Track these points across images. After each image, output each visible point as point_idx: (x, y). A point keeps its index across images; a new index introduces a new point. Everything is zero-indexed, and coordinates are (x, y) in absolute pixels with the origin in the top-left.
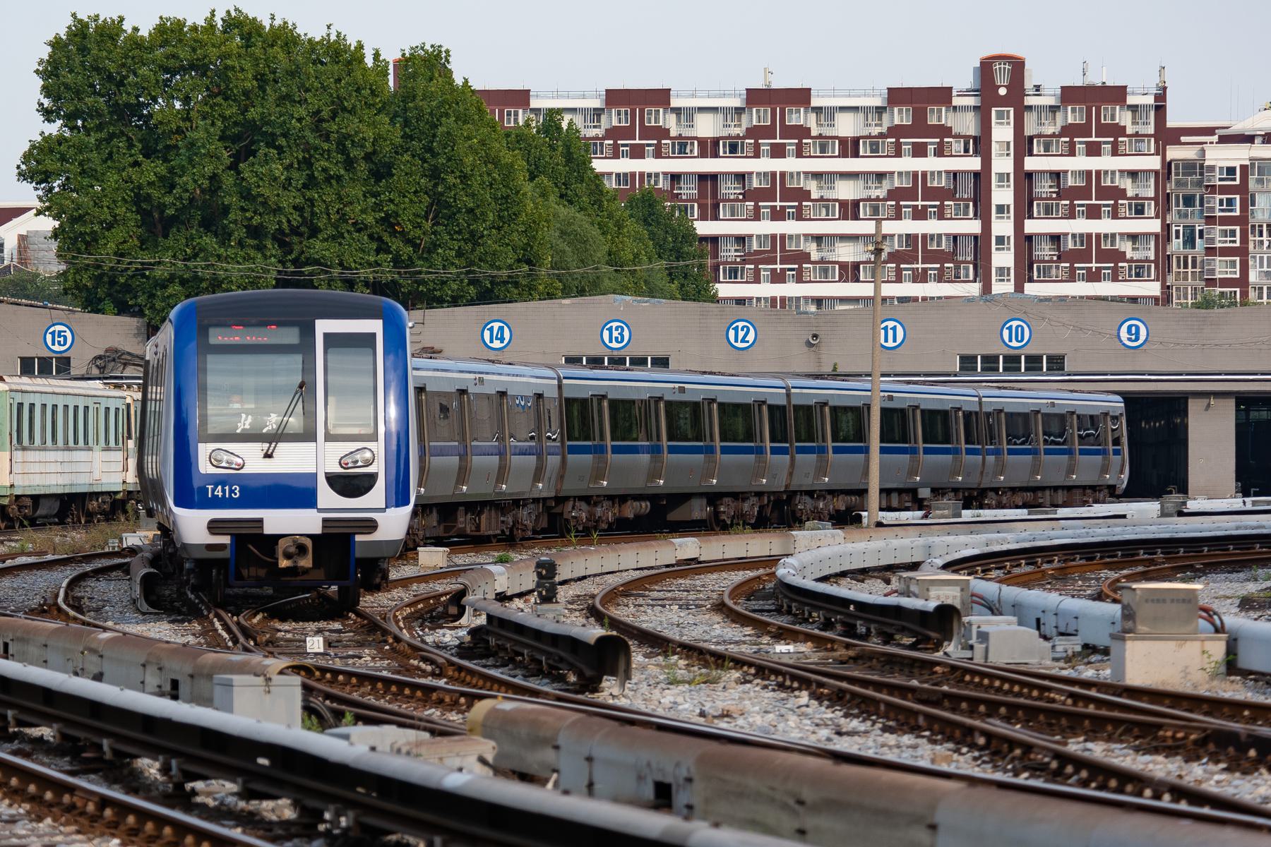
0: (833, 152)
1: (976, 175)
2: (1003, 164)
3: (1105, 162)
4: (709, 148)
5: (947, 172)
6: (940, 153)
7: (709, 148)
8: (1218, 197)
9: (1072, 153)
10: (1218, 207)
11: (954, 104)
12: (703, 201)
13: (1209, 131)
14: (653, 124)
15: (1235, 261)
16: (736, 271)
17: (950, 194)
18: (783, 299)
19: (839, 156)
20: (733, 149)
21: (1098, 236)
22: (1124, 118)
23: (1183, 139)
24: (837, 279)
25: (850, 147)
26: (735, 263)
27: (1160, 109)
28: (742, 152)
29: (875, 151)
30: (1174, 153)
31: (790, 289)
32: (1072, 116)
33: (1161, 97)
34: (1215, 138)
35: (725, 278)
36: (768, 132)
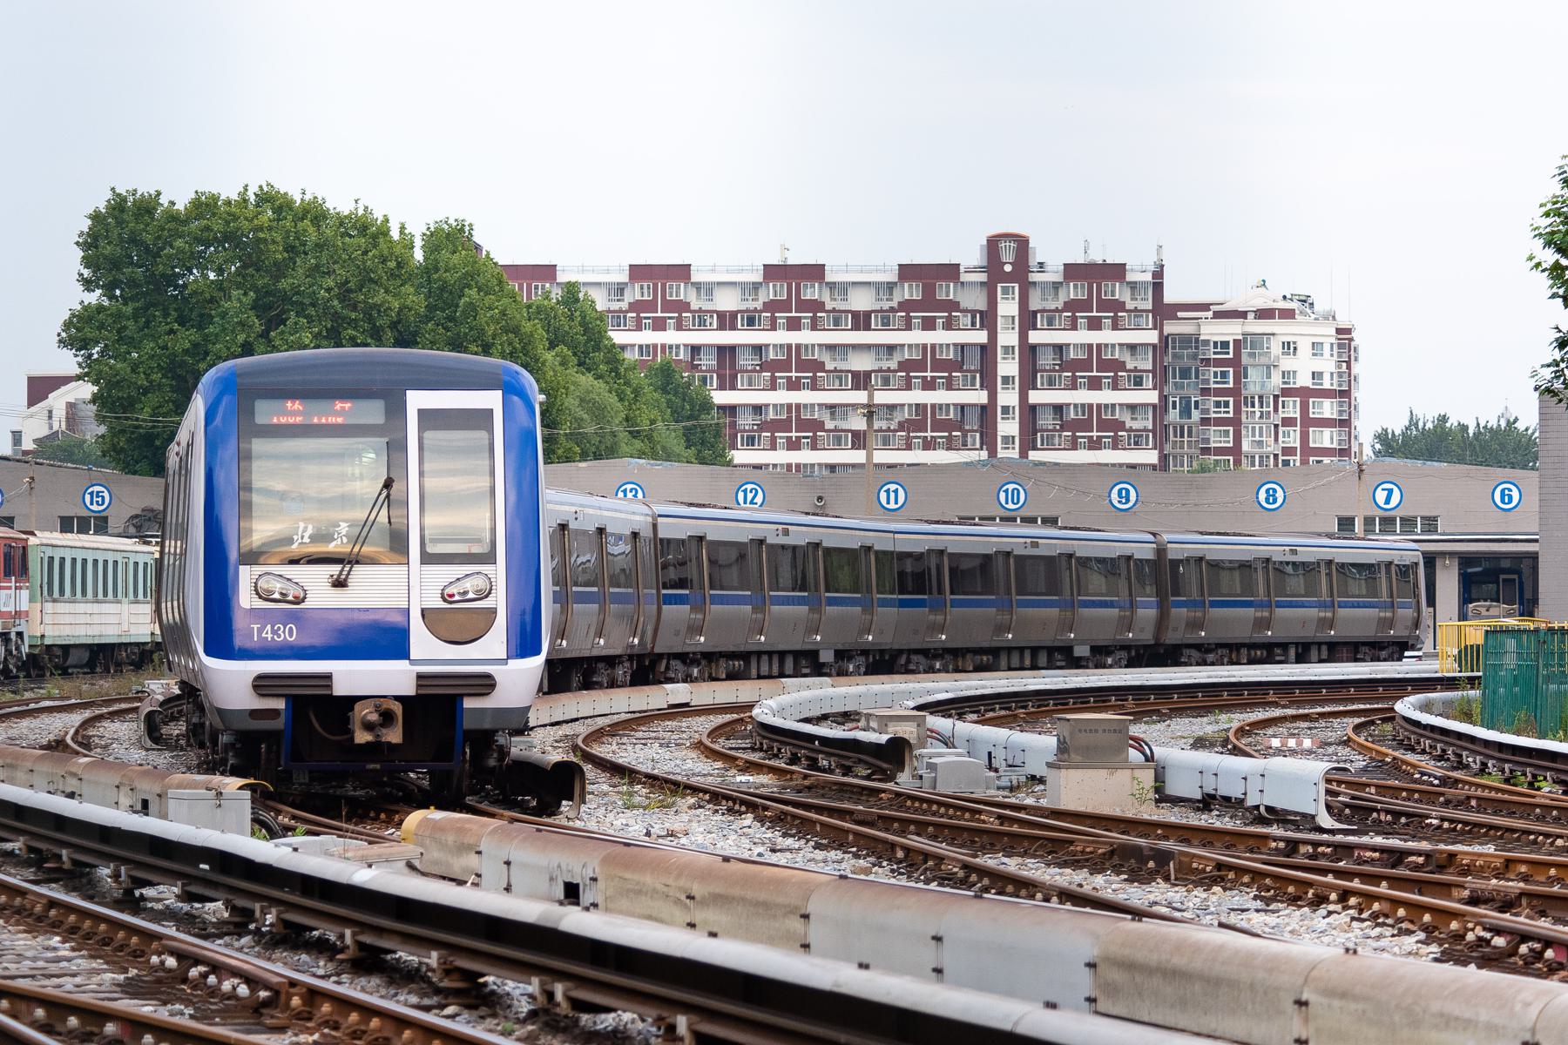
0: (846, 325)
1: (983, 347)
2: (1008, 337)
3: (1106, 336)
4: (727, 321)
5: (955, 345)
6: (949, 326)
7: (727, 321)
8: (1213, 369)
10: (1213, 380)
11: (961, 280)
12: (722, 372)
13: (1204, 307)
14: (674, 298)
15: (1228, 431)
16: (753, 438)
17: (958, 365)
18: (798, 466)
19: (852, 330)
20: (751, 322)
21: (1099, 406)
22: (1120, 293)
23: (1180, 314)
24: (850, 447)
25: (861, 321)
26: (753, 431)
27: (1158, 287)
28: (760, 325)
29: (886, 324)
30: (1170, 328)
31: (805, 456)
32: (1073, 292)
33: (1158, 274)
34: (1210, 314)
35: (742, 445)
36: (784, 306)
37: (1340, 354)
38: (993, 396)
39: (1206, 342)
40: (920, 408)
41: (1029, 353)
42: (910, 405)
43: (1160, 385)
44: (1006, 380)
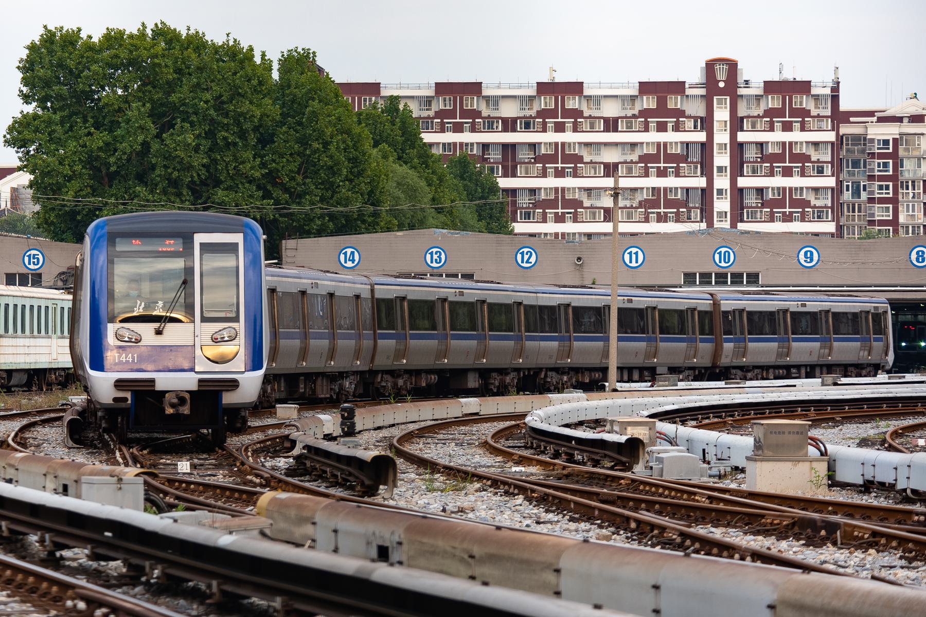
3: (796, 136)
9: (772, 129)
21: (791, 189)
32: (773, 102)
38: (710, 182)
41: (738, 149)
43: (837, 172)
44: (720, 169)
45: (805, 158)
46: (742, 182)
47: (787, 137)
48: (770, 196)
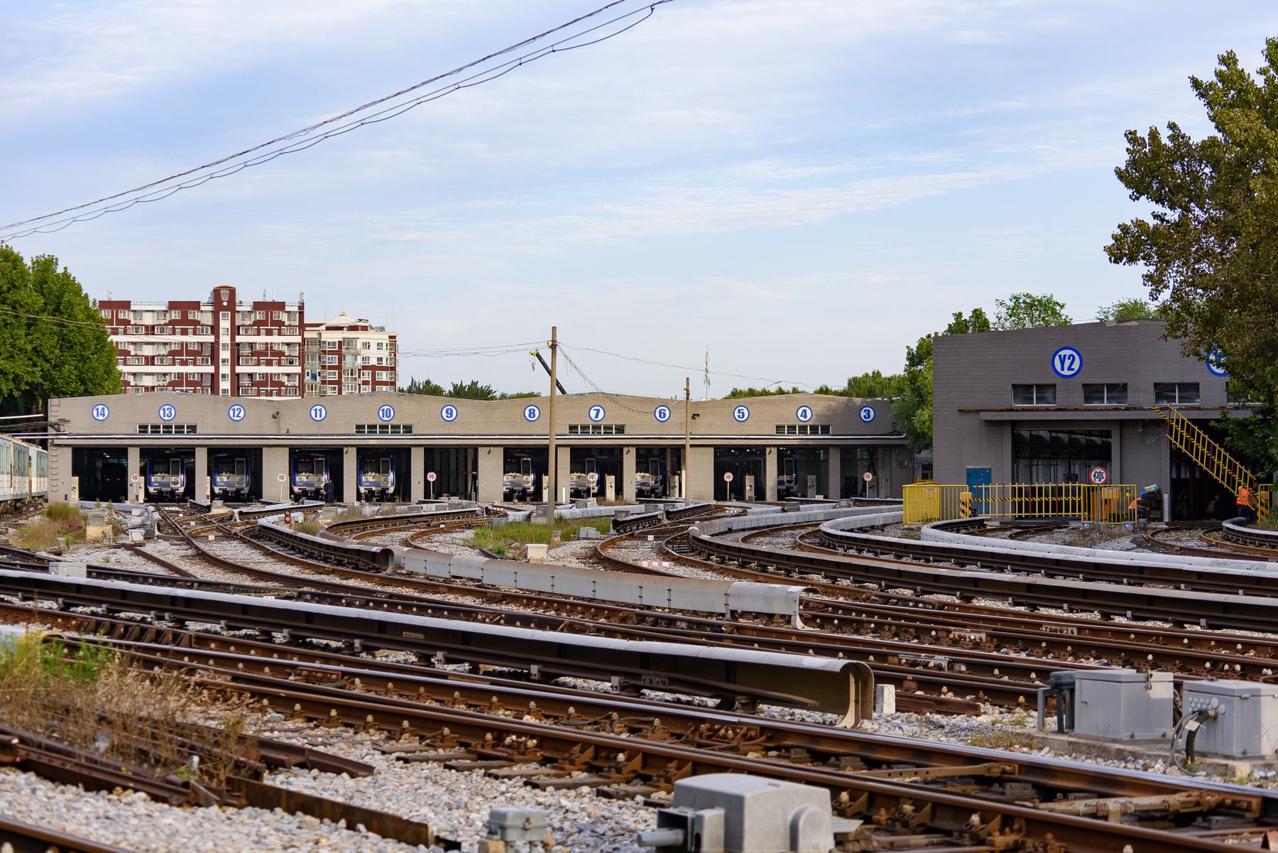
37: (391, 349)
38: (217, 369)
39: (324, 342)
40: (180, 375)
41: (236, 348)
42: (175, 374)
44: (224, 361)
45: (281, 354)
46: (239, 369)
47: (269, 339)
48: (258, 379)
